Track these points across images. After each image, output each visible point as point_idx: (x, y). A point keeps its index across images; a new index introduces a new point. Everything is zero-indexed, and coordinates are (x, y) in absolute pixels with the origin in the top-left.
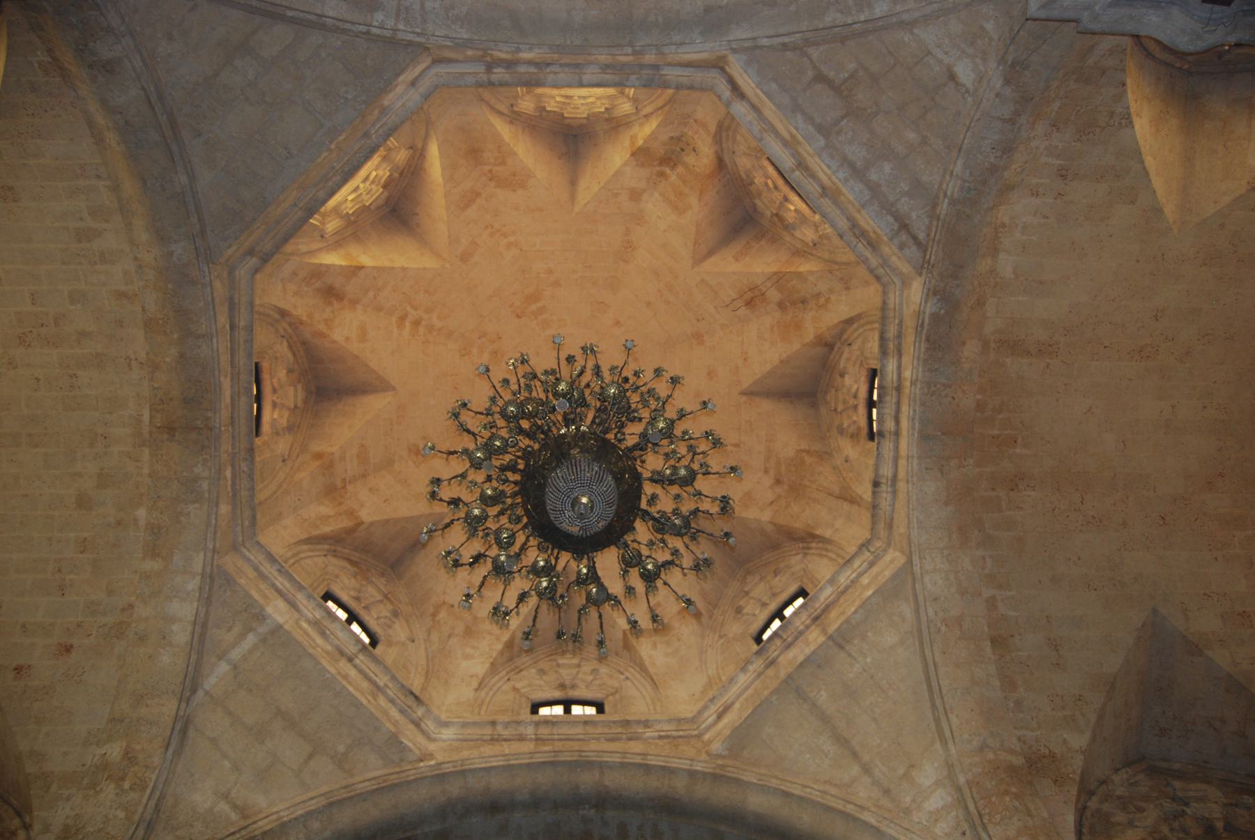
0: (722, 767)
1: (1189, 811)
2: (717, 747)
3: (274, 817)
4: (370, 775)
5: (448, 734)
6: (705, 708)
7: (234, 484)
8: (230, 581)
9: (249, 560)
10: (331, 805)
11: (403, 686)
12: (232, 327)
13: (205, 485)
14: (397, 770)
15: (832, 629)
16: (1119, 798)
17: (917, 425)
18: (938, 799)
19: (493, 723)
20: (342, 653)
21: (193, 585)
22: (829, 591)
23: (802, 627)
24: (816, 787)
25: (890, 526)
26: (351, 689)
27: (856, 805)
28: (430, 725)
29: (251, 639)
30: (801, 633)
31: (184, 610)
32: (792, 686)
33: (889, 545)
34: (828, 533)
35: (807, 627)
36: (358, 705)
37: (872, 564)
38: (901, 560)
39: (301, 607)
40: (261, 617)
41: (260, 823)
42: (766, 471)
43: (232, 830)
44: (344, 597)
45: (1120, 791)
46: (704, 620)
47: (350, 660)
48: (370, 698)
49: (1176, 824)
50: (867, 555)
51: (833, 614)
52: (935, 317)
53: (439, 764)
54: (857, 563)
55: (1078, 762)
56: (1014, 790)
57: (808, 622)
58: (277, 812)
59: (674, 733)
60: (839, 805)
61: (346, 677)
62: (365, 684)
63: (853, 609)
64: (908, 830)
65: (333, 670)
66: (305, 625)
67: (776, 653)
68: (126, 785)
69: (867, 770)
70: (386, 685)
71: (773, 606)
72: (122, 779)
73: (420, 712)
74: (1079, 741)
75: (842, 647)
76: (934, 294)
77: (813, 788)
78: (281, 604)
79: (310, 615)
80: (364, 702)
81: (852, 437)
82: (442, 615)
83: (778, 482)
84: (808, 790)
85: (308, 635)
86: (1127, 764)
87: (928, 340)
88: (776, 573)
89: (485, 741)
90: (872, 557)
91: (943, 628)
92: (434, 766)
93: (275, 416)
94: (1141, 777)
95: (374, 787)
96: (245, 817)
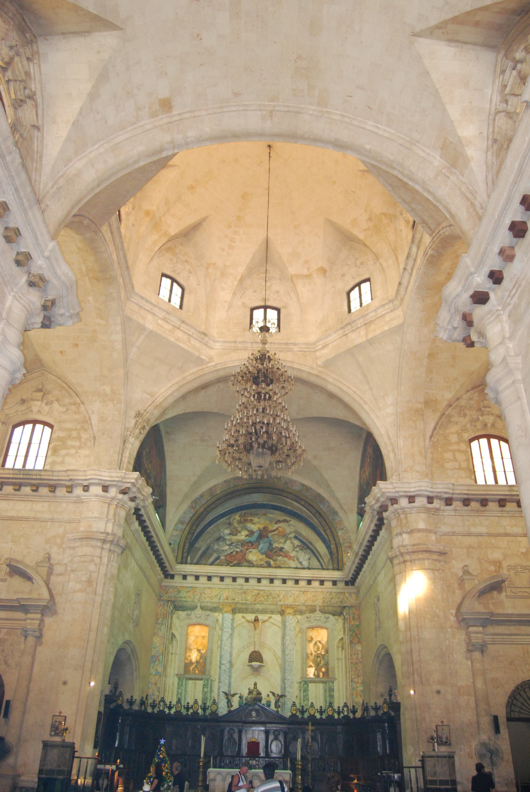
0: (320, 372)
1: (481, 418)
2: (320, 362)
3: (162, 396)
4: (192, 371)
5: (218, 346)
6: (318, 341)
7: (123, 282)
8: (130, 319)
9: (134, 302)
10: (180, 387)
11: (199, 332)
12: (112, 233)
13: (115, 295)
14: (200, 368)
15: (370, 336)
16: (461, 407)
17: (417, 283)
18: (390, 410)
19: (235, 342)
20: (175, 327)
21: (119, 328)
22: (373, 314)
23: (359, 325)
24: (353, 388)
25: (402, 300)
26: (181, 344)
27: (364, 401)
28: (211, 342)
29: (142, 337)
30: (359, 328)
31: (118, 337)
32: (351, 352)
33: (401, 305)
34: (385, 265)
35: (362, 326)
36: (184, 349)
37: (392, 311)
38: (401, 321)
39: (157, 314)
40: (144, 329)
41: (158, 399)
42: (366, 211)
43: (150, 403)
44: (168, 273)
45: (463, 402)
46: (327, 274)
47: (179, 328)
48: (188, 343)
49: (473, 424)
50: (391, 305)
51: (372, 327)
52: (432, 256)
53: (216, 365)
54: (386, 307)
55: (445, 404)
56: (414, 419)
57: (362, 324)
58: (162, 393)
59: (305, 350)
60: (358, 399)
61: (178, 339)
62: (185, 337)
63: (378, 332)
64: (378, 417)
65: (173, 339)
66: (160, 321)
67: (347, 332)
68: (115, 402)
69: (371, 389)
70: (193, 333)
71: (357, 281)
72: (114, 400)
73: (206, 339)
74: (449, 396)
75: (371, 344)
76: (433, 249)
77: (351, 389)
78: (150, 317)
79: (161, 316)
80: (186, 347)
81: (406, 221)
82: (211, 270)
83: (370, 219)
84: (349, 389)
85: (162, 326)
86: (473, 389)
87: (427, 260)
88: (362, 264)
89: (232, 349)
90: (392, 308)
91: (409, 354)
92: (214, 366)
93: (127, 210)
94: (476, 394)
95: (194, 377)
96: (152, 396)
